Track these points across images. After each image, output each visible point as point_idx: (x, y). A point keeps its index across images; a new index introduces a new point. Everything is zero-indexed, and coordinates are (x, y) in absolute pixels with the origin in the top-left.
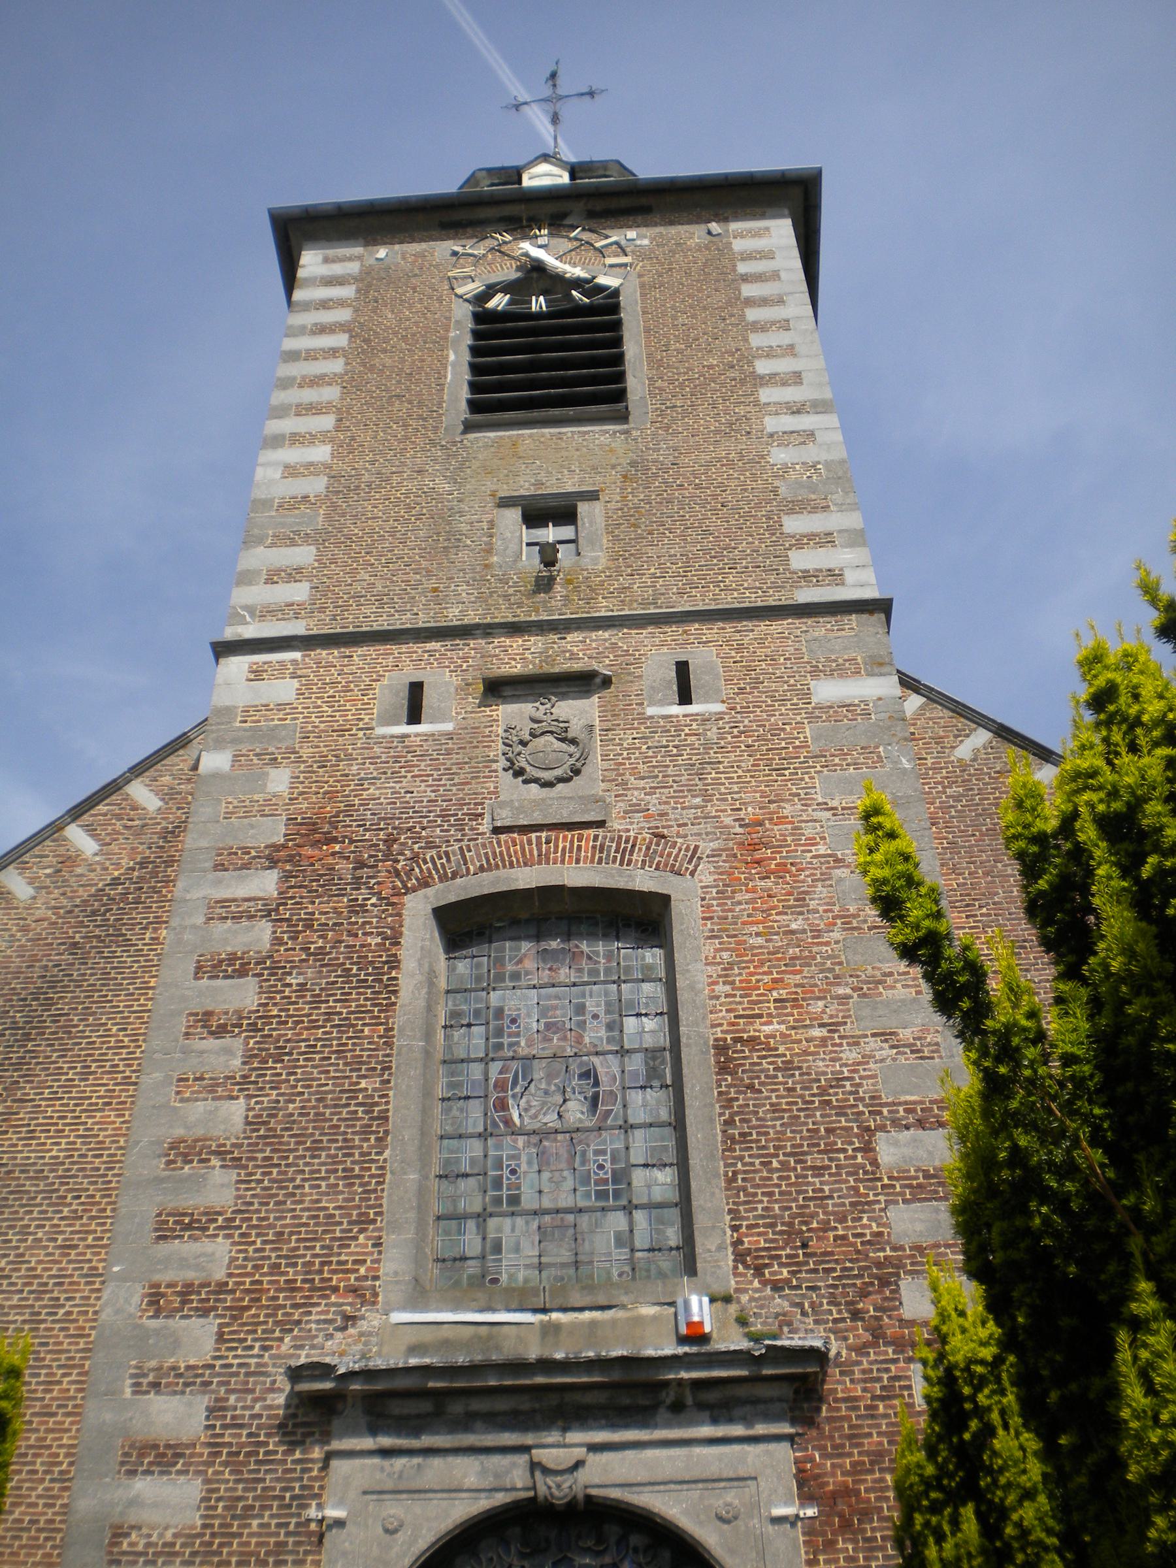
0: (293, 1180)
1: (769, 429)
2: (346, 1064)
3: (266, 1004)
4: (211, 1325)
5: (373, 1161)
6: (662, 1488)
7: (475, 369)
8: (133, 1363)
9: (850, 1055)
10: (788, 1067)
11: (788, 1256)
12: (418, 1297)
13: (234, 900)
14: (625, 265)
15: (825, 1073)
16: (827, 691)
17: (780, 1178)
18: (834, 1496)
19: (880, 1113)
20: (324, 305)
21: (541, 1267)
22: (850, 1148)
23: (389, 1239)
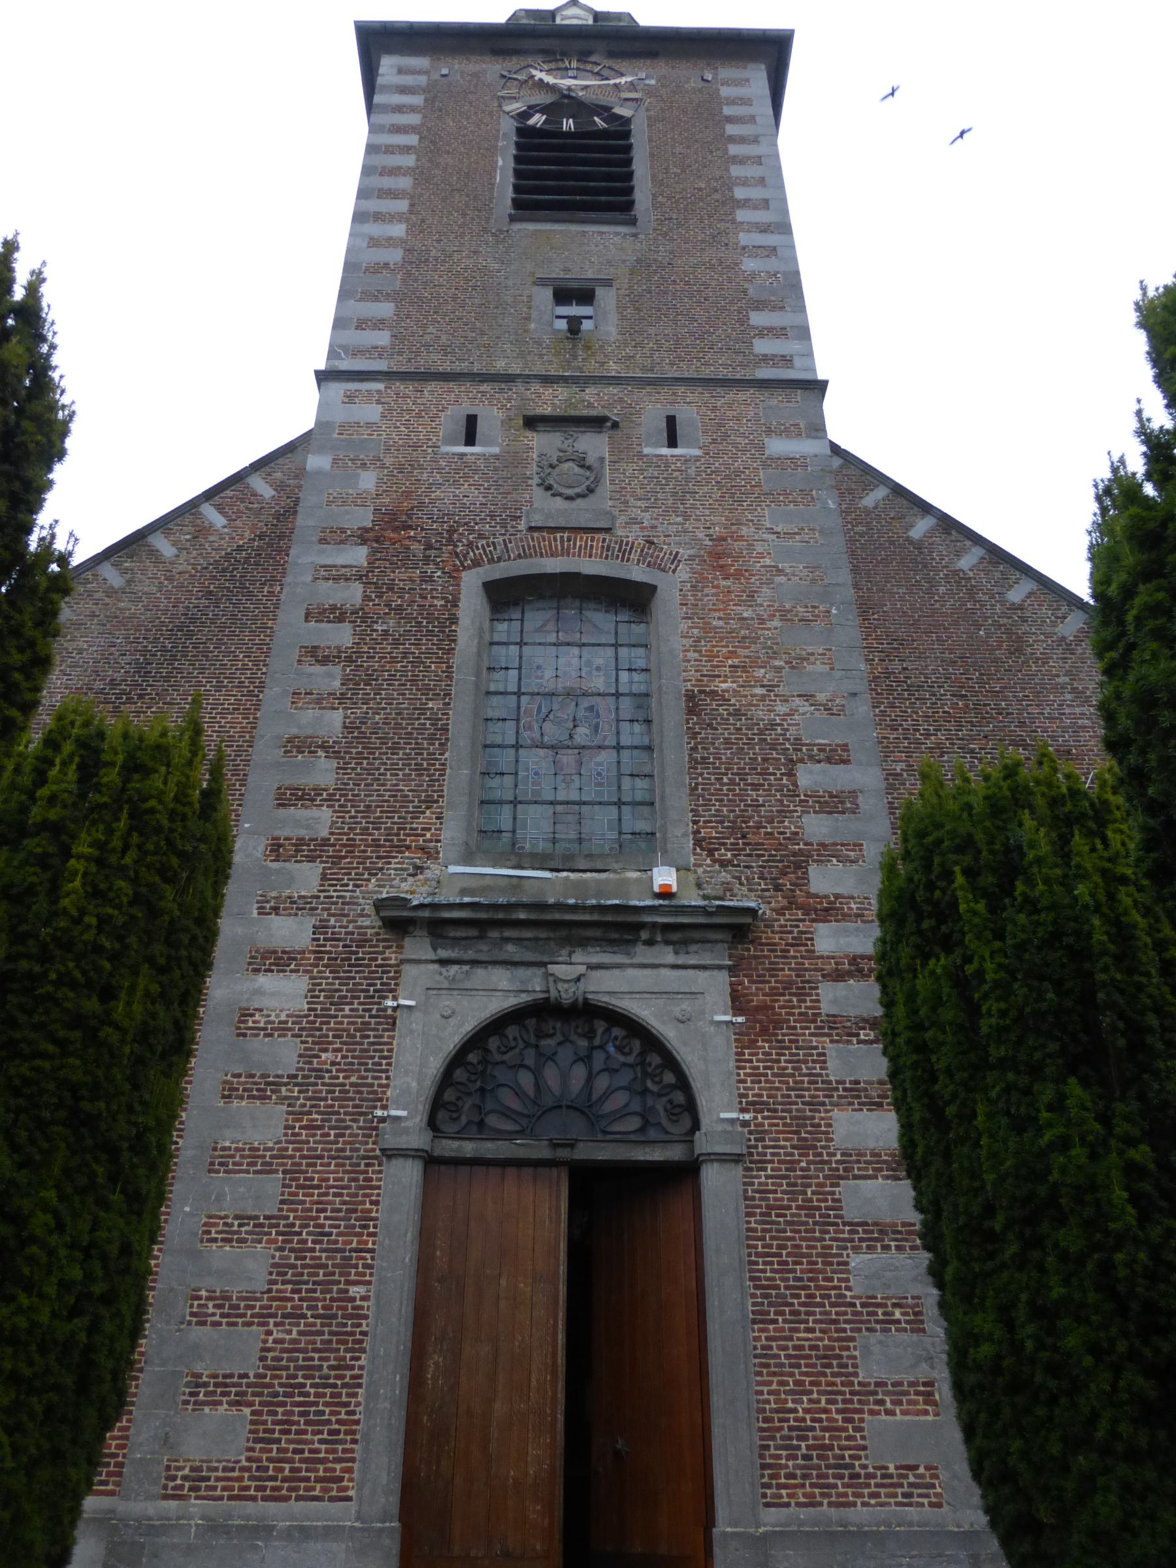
0: (378, 769)
1: (743, 243)
2: (417, 690)
3: (358, 644)
4: (317, 868)
5: (436, 759)
6: (638, 996)
7: (518, 174)
8: (260, 892)
9: (782, 708)
10: (737, 713)
11: (732, 844)
12: (468, 858)
13: (335, 566)
14: (636, 100)
15: (763, 720)
16: (777, 446)
17: (728, 790)
18: (758, 1009)
19: (801, 750)
20: (399, 109)
21: (554, 841)
22: (778, 773)
23: (447, 814)
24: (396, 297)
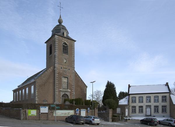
24: (58, 58)
